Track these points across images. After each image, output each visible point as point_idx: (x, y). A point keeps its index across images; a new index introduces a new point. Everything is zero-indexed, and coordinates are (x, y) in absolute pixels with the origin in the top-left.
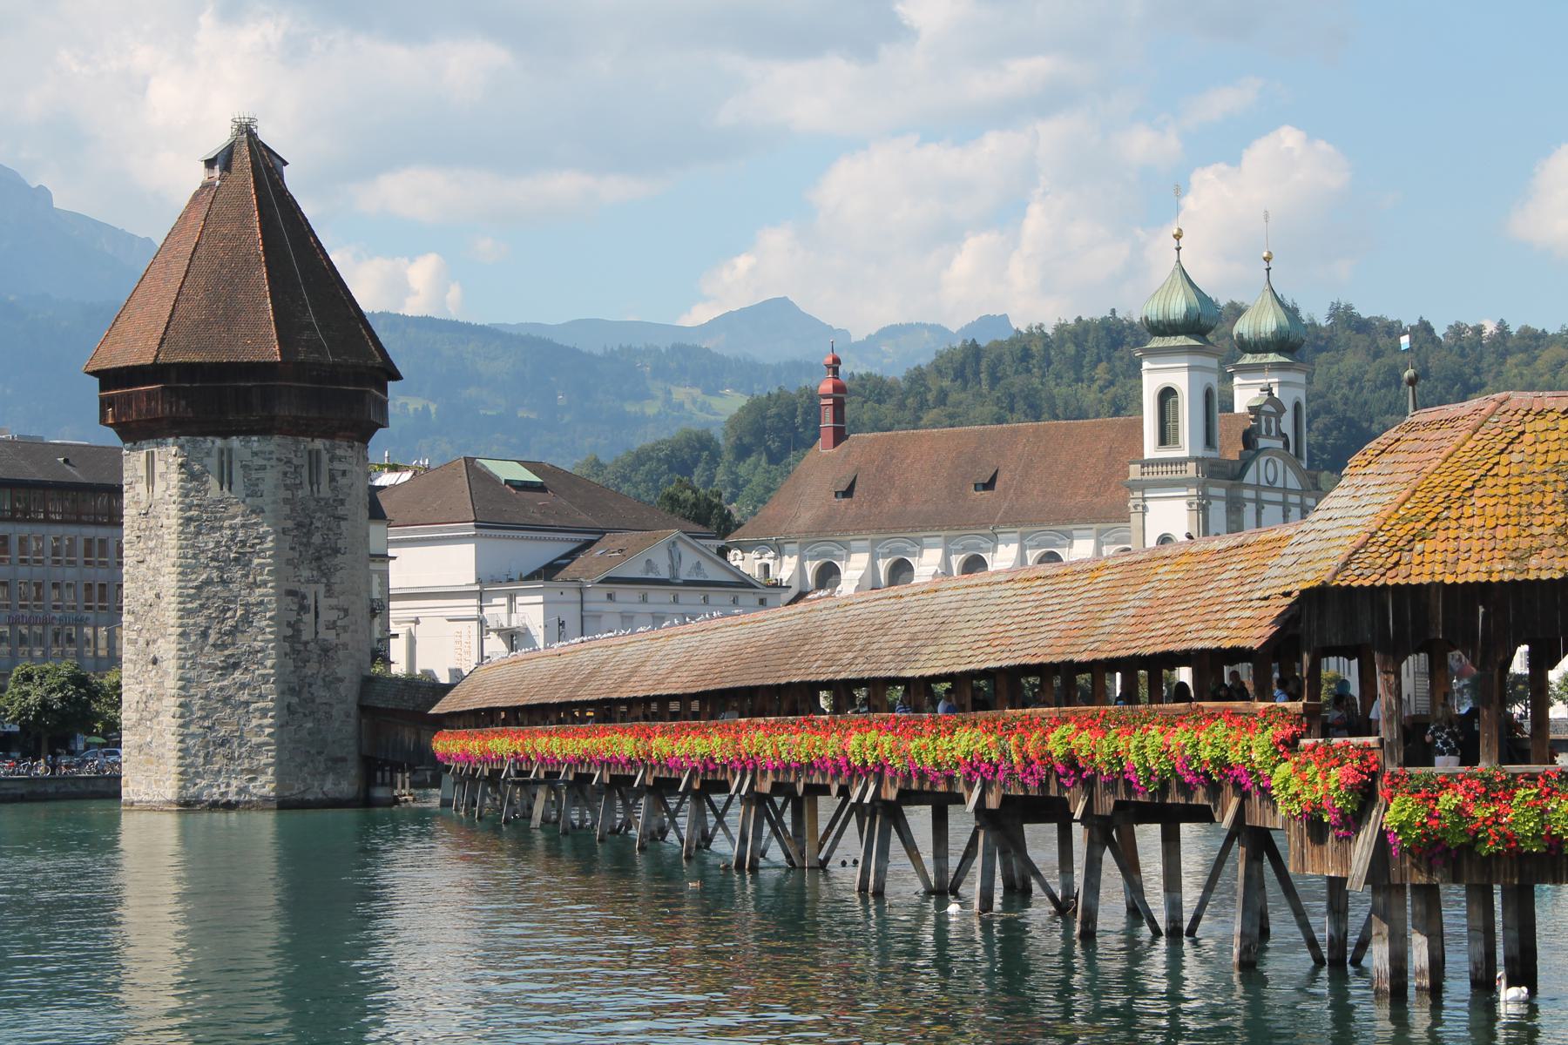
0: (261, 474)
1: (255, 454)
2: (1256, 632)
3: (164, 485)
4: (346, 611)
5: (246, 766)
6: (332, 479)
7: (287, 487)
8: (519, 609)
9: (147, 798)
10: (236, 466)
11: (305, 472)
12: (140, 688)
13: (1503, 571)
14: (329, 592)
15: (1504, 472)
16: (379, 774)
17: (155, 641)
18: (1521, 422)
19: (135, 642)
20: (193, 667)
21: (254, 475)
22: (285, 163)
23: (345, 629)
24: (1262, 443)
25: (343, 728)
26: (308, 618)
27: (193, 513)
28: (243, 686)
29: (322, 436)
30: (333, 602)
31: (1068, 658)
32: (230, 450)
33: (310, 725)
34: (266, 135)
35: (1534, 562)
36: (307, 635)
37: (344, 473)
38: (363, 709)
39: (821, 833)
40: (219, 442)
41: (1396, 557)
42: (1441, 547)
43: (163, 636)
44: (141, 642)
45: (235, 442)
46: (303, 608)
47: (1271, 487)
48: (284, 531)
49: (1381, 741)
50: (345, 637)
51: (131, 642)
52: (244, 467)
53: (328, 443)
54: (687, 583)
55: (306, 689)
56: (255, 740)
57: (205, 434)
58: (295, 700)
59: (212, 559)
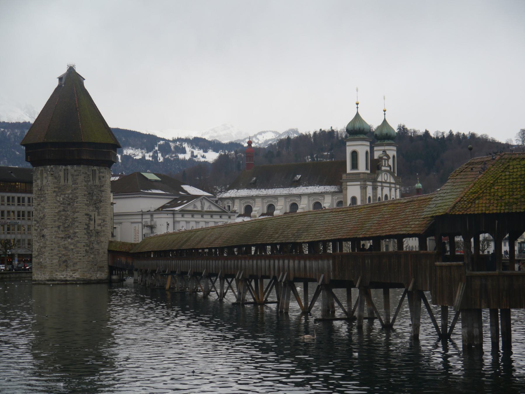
0: (77, 177)
1: (75, 171)
2: (422, 229)
4: (104, 221)
5: (72, 268)
6: (100, 179)
7: (85, 181)
8: (155, 220)
10: (69, 174)
11: (91, 177)
12: (38, 244)
13: (504, 209)
14: (99, 215)
15: (503, 178)
16: (114, 272)
17: (43, 230)
18: (508, 162)
20: (55, 237)
21: (75, 177)
22: (84, 79)
23: (104, 226)
24: (383, 168)
25: (104, 259)
26: (92, 222)
27: (56, 189)
28: (71, 244)
29: (97, 165)
30: (100, 217)
31: (355, 236)
32: (67, 169)
33: (92, 256)
34: (78, 70)
35: (514, 206)
36: (92, 228)
37: (103, 177)
38: (109, 251)
39: (264, 290)
40: (64, 167)
41: (470, 205)
42: (484, 202)
43: (46, 228)
44: (39, 230)
45: (69, 167)
46: (90, 219)
47: (386, 182)
48: (85, 195)
49: (464, 264)
50: (104, 228)
51: (36, 230)
52: (72, 175)
53: (98, 167)
54: (206, 212)
55: (91, 245)
56: (75, 261)
57: (59, 164)
58: (88, 248)
59: (61, 204)
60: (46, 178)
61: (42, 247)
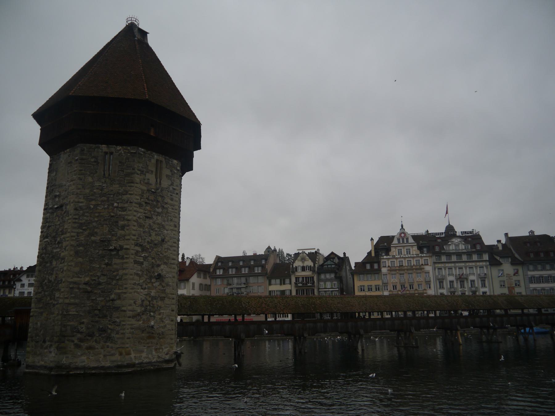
9: (148, 360)
17: (159, 266)
19: (142, 263)
43: (166, 263)
60: (167, 176)
61: (154, 298)
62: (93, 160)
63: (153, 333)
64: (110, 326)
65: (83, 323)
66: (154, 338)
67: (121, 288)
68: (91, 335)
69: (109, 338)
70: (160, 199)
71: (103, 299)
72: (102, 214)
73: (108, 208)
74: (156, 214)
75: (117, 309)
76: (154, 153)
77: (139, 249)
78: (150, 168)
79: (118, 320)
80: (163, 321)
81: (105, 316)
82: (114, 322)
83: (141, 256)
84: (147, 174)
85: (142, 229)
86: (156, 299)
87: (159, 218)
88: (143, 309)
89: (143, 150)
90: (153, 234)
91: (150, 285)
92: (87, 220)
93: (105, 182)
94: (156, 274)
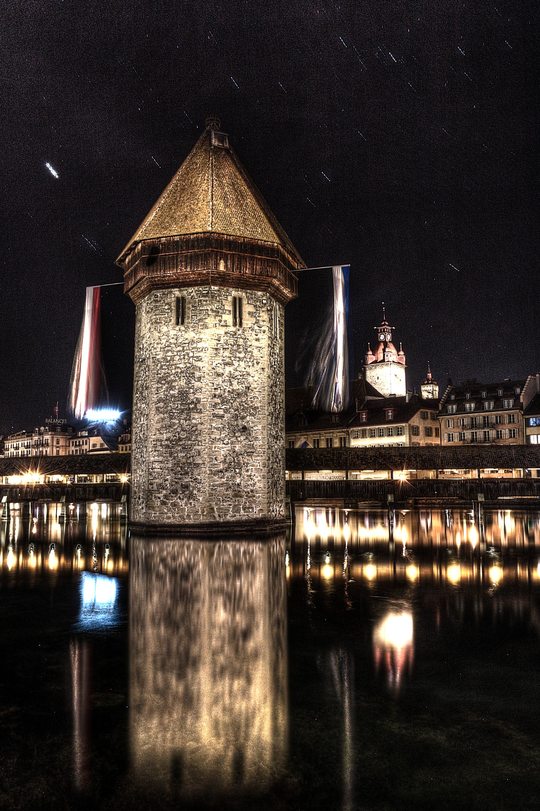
3: (254, 320)
17: (243, 418)
43: (251, 415)
60: (249, 313)
62: (166, 307)
63: (239, 491)
64: (191, 484)
65: (167, 480)
66: (241, 497)
67: (200, 443)
68: (175, 492)
69: (191, 496)
70: (241, 342)
71: (184, 455)
72: (178, 366)
73: (184, 358)
74: (238, 359)
75: (197, 465)
76: (231, 289)
77: (218, 401)
78: (226, 308)
79: (199, 477)
80: (252, 479)
81: (187, 473)
82: (194, 479)
83: (220, 408)
84: (223, 315)
85: (220, 378)
86: (241, 454)
87: (242, 364)
88: (226, 465)
89: (216, 288)
90: (235, 382)
91: (233, 439)
92: (165, 374)
93: (180, 330)
94: (241, 427)
